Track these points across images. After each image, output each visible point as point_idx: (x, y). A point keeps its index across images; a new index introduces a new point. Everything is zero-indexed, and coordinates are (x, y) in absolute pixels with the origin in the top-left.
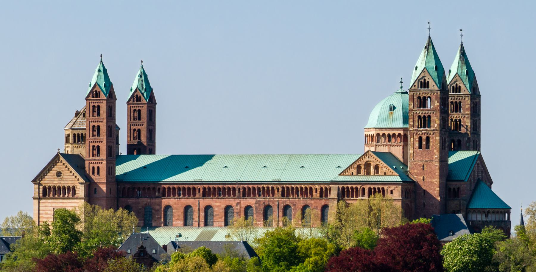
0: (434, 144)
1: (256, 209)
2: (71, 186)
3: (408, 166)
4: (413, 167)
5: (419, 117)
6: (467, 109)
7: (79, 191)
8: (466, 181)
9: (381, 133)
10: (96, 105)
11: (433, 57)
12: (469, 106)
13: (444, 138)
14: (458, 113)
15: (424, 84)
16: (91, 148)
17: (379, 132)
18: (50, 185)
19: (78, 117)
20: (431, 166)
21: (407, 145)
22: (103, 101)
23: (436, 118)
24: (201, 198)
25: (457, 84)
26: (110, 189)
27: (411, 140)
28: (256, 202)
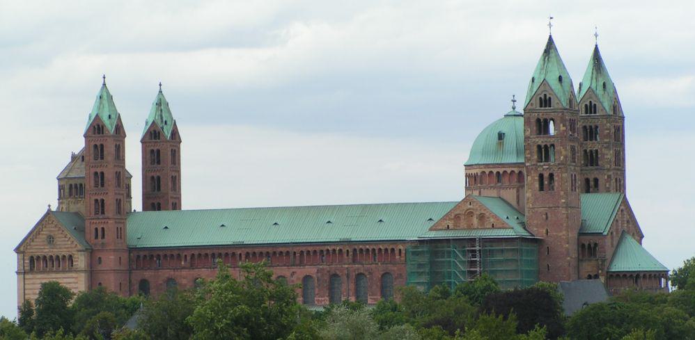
3: (524, 215)
7: (77, 261)
8: (605, 233)
9: (487, 171)
10: (98, 144)
11: (555, 64)
14: (594, 141)
15: (546, 102)
17: (484, 170)
18: (39, 254)
21: (524, 186)
22: (108, 139)
26: (120, 258)
27: (528, 179)
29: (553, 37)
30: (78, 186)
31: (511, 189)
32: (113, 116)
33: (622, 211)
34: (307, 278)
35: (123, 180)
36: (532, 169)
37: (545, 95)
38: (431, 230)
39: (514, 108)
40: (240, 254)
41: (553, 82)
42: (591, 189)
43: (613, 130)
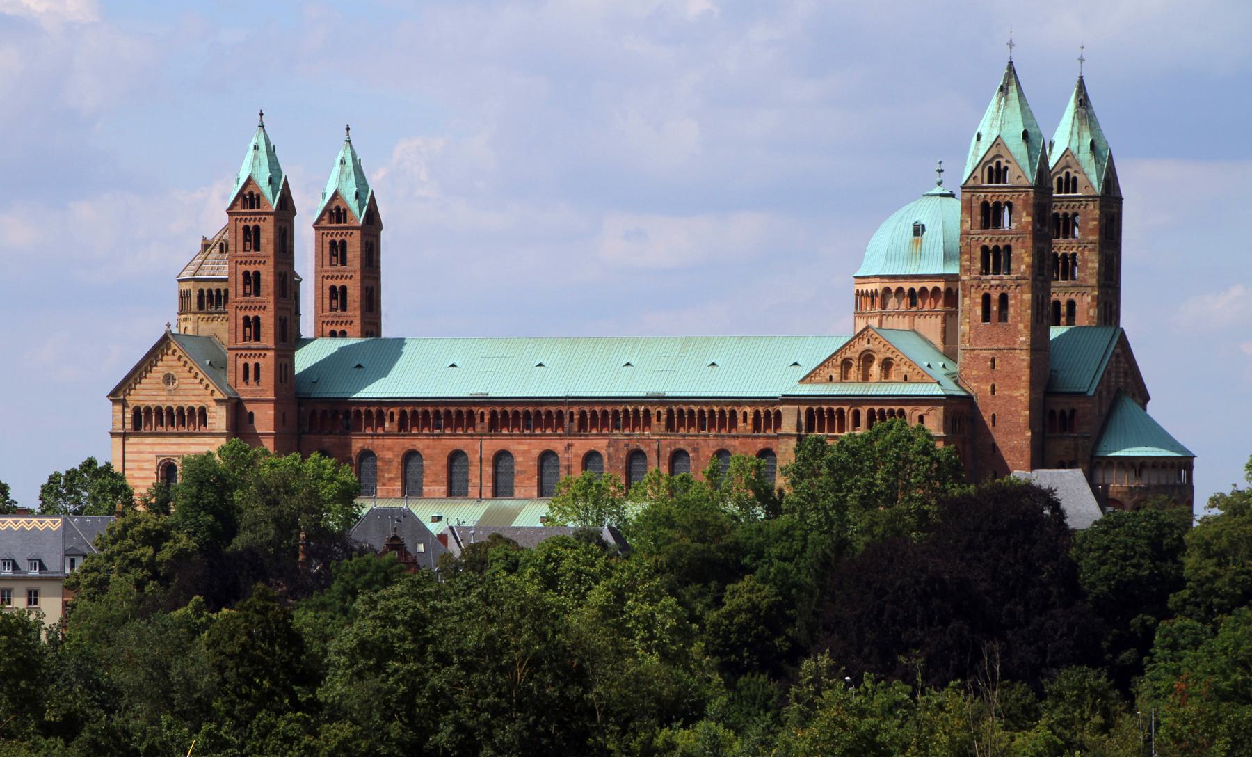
0: (1019, 311)
1: (609, 459)
2: (197, 408)
4: (969, 364)
6: (1091, 231)
7: (214, 418)
8: (1091, 393)
9: (894, 287)
11: (1018, 110)
12: (1095, 223)
13: (1040, 296)
14: (1070, 239)
15: (997, 173)
16: (241, 322)
18: (150, 404)
19: (207, 252)
20: (1010, 361)
22: (267, 217)
24: (485, 435)
25: (1068, 174)
26: (284, 414)
27: (964, 303)
28: (609, 443)
30: (214, 293)
31: (933, 317)
33: (1117, 356)
34: (591, 458)
35: (287, 286)
38: (802, 381)
42: (1063, 320)
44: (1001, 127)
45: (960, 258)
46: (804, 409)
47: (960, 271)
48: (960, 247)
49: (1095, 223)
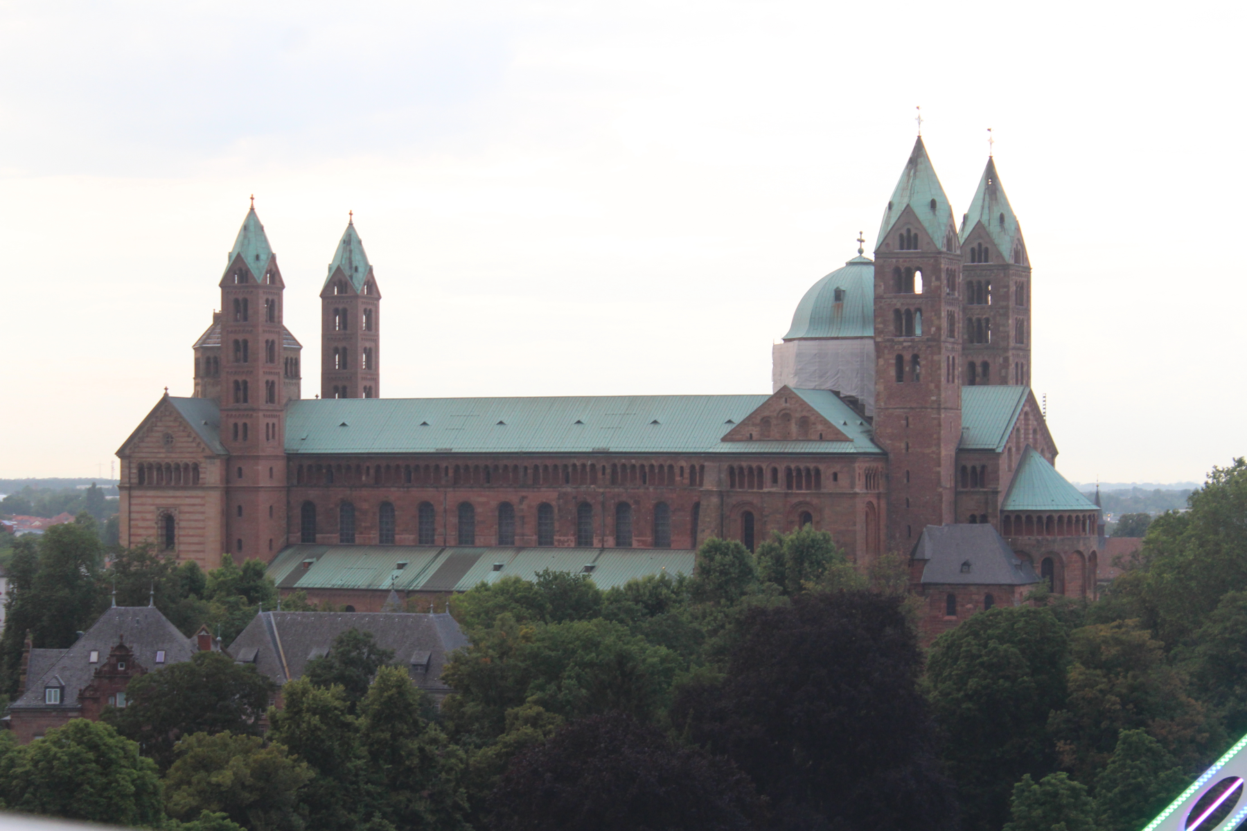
1: (559, 510)
5: (897, 312)
7: (205, 473)
12: (1005, 290)
16: (232, 385)
23: (933, 314)
25: (980, 245)
28: (559, 495)
29: (922, 138)
32: (263, 257)
33: (1026, 414)
36: (885, 347)
37: (909, 231)
38: (724, 439)
39: (861, 251)
40: (447, 468)
41: (922, 213)
42: (978, 379)
43: (1013, 289)
44: (910, 197)
45: (875, 321)
46: (725, 465)
47: (875, 333)
48: (875, 310)
49: (1005, 290)
